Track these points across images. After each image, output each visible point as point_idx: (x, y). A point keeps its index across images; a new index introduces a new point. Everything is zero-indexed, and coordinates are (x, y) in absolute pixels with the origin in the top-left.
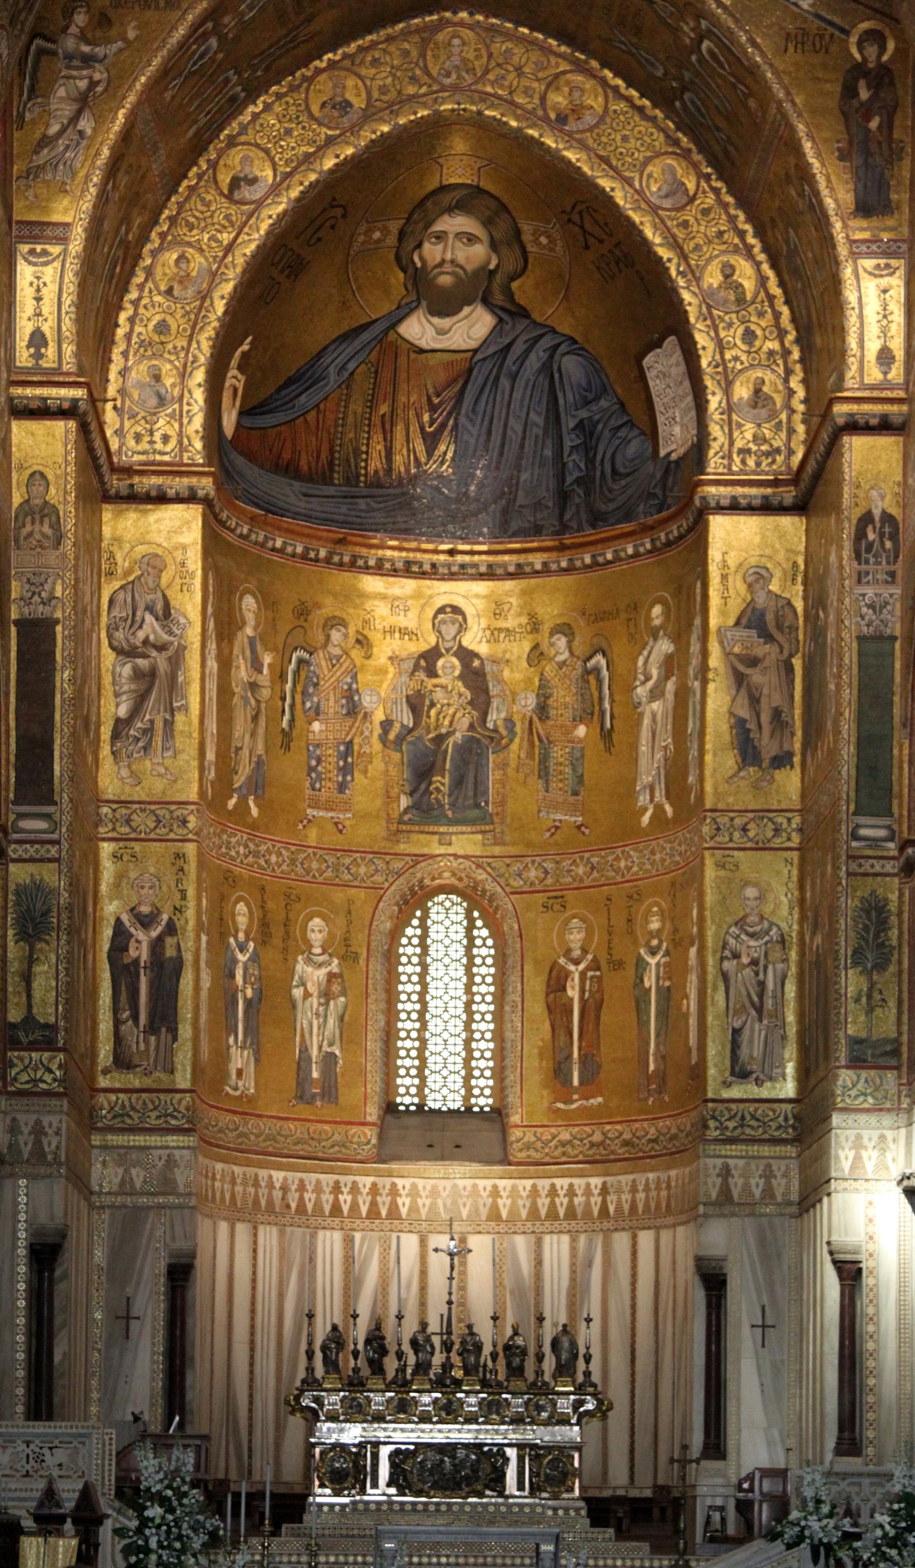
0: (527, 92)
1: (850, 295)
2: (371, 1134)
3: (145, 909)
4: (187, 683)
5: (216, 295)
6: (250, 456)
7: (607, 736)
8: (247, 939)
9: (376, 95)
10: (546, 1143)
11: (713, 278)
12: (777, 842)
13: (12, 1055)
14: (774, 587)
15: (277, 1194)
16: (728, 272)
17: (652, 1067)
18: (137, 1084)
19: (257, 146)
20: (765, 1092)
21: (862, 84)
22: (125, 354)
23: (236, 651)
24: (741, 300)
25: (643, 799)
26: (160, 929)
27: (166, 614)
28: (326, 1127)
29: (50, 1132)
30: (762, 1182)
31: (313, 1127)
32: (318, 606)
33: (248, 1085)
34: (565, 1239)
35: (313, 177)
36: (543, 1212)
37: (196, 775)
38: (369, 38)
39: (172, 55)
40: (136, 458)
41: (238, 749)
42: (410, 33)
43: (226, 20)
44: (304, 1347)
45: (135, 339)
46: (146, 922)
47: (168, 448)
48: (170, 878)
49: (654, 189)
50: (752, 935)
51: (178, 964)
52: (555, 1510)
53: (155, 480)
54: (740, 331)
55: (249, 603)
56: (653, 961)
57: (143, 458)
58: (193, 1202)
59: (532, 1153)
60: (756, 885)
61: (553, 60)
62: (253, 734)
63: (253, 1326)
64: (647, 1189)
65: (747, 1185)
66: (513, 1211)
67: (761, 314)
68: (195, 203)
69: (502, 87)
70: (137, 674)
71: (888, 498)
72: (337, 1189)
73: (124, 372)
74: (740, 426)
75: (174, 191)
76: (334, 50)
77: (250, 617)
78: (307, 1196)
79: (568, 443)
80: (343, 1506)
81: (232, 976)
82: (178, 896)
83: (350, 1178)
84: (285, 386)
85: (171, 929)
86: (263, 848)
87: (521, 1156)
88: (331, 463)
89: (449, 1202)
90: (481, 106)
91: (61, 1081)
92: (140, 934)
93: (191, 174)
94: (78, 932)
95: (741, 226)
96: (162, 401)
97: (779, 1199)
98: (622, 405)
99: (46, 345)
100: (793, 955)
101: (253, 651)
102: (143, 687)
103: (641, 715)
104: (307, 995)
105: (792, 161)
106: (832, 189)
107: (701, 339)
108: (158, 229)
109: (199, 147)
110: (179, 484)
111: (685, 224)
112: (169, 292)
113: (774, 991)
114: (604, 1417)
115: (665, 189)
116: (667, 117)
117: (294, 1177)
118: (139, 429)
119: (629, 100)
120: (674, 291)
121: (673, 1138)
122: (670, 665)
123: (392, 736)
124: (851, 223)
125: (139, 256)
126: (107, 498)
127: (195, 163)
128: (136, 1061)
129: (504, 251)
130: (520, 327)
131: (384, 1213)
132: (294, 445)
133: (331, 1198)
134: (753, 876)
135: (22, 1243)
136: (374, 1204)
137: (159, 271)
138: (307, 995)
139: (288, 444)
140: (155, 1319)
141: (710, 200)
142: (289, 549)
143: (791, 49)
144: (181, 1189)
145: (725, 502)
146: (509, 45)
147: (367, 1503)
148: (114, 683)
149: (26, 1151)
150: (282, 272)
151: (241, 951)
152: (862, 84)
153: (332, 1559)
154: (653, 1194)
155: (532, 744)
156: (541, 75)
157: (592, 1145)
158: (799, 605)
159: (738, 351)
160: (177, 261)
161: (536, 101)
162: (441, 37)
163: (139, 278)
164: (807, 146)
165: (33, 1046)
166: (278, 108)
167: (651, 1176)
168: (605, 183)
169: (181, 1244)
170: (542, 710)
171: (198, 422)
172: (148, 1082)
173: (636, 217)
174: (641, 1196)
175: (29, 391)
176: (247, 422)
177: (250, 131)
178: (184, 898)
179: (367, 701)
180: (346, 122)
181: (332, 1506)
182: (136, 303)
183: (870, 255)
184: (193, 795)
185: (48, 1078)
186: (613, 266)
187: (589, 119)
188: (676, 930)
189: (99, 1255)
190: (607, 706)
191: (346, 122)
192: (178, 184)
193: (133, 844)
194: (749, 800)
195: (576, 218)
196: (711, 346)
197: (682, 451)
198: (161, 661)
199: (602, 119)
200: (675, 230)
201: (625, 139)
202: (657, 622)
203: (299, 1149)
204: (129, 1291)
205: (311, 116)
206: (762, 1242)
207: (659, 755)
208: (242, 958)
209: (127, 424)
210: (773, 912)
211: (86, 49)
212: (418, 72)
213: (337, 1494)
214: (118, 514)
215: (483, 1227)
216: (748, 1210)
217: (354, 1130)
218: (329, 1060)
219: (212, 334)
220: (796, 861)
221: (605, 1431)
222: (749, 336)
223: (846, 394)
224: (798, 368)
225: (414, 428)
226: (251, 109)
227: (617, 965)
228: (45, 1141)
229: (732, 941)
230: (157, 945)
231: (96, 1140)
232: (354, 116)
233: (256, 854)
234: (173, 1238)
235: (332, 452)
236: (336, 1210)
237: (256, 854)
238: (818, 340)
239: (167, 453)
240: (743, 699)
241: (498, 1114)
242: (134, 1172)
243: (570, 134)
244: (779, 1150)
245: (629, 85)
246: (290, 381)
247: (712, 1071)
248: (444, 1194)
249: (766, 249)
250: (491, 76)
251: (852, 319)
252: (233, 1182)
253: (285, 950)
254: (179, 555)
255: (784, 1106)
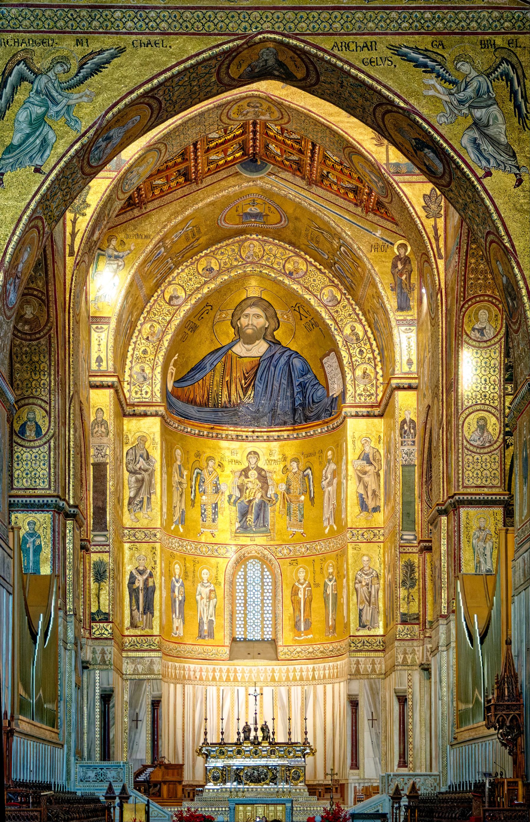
0: (279, 264)
1: (396, 339)
2: (227, 650)
3: (141, 568)
4: (155, 484)
5: (165, 340)
6: (178, 398)
7: (312, 499)
8: (179, 578)
9: (222, 265)
10: (291, 652)
11: (347, 331)
12: (375, 539)
13: (93, 624)
14: (372, 445)
15: (192, 673)
16: (353, 329)
17: (330, 624)
18: (139, 633)
19: (179, 285)
20: (371, 633)
21: (399, 263)
22: (131, 362)
23: (174, 470)
24: (358, 339)
25: (326, 523)
26: (147, 575)
27: (148, 458)
28: (210, 647)
29: (107, 653)
30: (371, 666)
31: (205, 647)
32: (204, 453)
33: (181, 632)
34: (300, 688)
35: (200, 296)
36: (291, 678)
37: (160, 518)
38: (219, 245)
39: (147, 255)
40: (136, 400)
41: (175, 507)
42: (235, 243)
43: (167, 241)
44: (203, 731)
45: (135, 356)
46: (141, 573)
47: (148, 396)
48: (150, 556)
49: (325, 298)
50: (366, 575)
51: (154, 589)
52: (296, 789)
53: (143, 408)
54: (358, 350)
55: (178, 452)
56: (330, 584)
57: (138, 400)
58: (161, 677)
59: (287, 656)
60: (367, 555)
61: (287, 252)
62: (180, 501)
63: (184, 723)
64: (329, 669)
65: (365, 667)
66: (280, 678)
67: (365, 344)
68: (156, 305)
69: (269, 262)
70: (137, 481)
71: (412, 414)
72: (214, 671)
73: (130, 369)
74: (358, 385)
75: (148, 301)
76: (207, 249)
77: (179, 457)
78: (203, 673)
79: (296, 391)
80: (218, 789)
81: (174, 591)
82: (153, 563)
83: (220, 667)
84: (191, 371)
85: (151, 575)
86: (185, 543)
87: (283, 657)
88: (208, 399)
89: (256, 675)
90: (261, 269)
91: (112, 634)
92: (139, 577)
93: (155, 295)
94: (117, 578)
95: (357, 312)
96: (145, 379)
97: (378, 672)
98: (316, 377)
99: (102, 361)
100: (382, 582)
101: (180, 470)
102: (139, 485)
103: (324, 492)
104: (202, 598)
105: (375, 291)
106: (389, 301)
107: (344, 353)
108: (143, 316)
109: (158, 285)
110: (152, 409)
111: (337, 312)
112: (147, 338)
113: (375, 595)
114: (313, 754)
115: (329, 299)
116: (329, 272)
117: (198, 667)
118: (136, 389)
119: (315, 266)
120: (333, 336)
121: (339, 650)
122: (335, 474)
123: (232, 500)
124: (396, 314)
125: (136, 326)
126: (125, 415)
127: (156, 291)
128: (139, 625)
129: (270, 320)
130: (277, 348)
131: (232, 679)
132: (194, 393)
133: (212, 674)
134: (365, 552)
135: (98, 694)
136: (228, 676)
137: (143, 331)
138: (202, 598)
139: (192, 393)
140: (147, 721)
141: (346, 302)
142: (193, 432)
143: (373, 251)
144: (156, 672)
145: (353, 414)
146: (271, 246)
147: (226, 788)
148: (129, 484)
149: (99, 660)
150: (189, 330)
151: (177, 582)
152: (399, 263)
153: (213, 809)
154: (332, 671)
155: (284, 503)
156: (283, 257)
157: (309, 653)
158: (382, 452)
159: (357, 358)
160: (150, 327)
161: (281, 267)
162: (246, 244)
163: (136, 333)
164: (380, 285)
165: (100, 621)
166: (186, 271)
167: (331, 664)
168: (307, 297)
169: (156, 693)
170: (288, 490)
171: (158, 386)
172: (143, 633)
173: (319, 309)
174: (327, 672)
175: (96, 379)
176: (177, 385)
177: (176, 279)
178: (155, 564)
179: (223, 488)
180: (212, 275)
181: (213, 789)
182: (135, 343)
183: (403, 325)
184: (159, 526)
185: (106, 633)
186: (311, 326)
187: (301, 273)
188: (338, 573)
189: (126, 697)
190: (312, 488)
191: (212, 275)
192: (150, 299)
193: (136, 544)
194: (363, 524)
195: (297, 309)
196: (347, 356)
197: (337, 394)
198: (146, 475)
199: (306, 273)
200: (333, 314)
201: (314, 280)
202: (330, 457)
203: (200, 656)
204: (137, 710)
205: (198, 273)
206: (371, 688)
207: (331, 507)
208: (177, 585)
209: (132, 388)
210: (374, 566)
211: (116, 253)
212: (238, 257)
213: (215, 785)
214: (129, 421)
215: (269, 684)
216: (366, 677)
217: (220, 648)
218: (211, 622)
219: (163, 354)
220: (382, 547)
221: (315, 759)
222: (361, 352)
223: (396, 376)
224: (379, 364)
225: (239, 386)
226: (177, 271)
227: (317, 585)
228: (106, 656)
229: (359, 577)
230: (146, 581)
231: (124, 654)
232: (214, 273)
233: (182, 546)
234: (154, 691)
235: (208, 395)
236: (214, 679)
237: (182, 546)
238: (386, 353)
239: (147, 398)
240: (361, 486)
241: (274, 642)
242: (138, 666)
243: (294, 279)
244: (377, 654)
245: (315, 261)
246: (193, 369)
247: (352, 625)
248: (254, 672)
249: (367, 320)
250: (265, 258)
251: (397, 349)
252: (175, 669)
253: (193, 582)
254: (152, 437)
255: (379, 638)
